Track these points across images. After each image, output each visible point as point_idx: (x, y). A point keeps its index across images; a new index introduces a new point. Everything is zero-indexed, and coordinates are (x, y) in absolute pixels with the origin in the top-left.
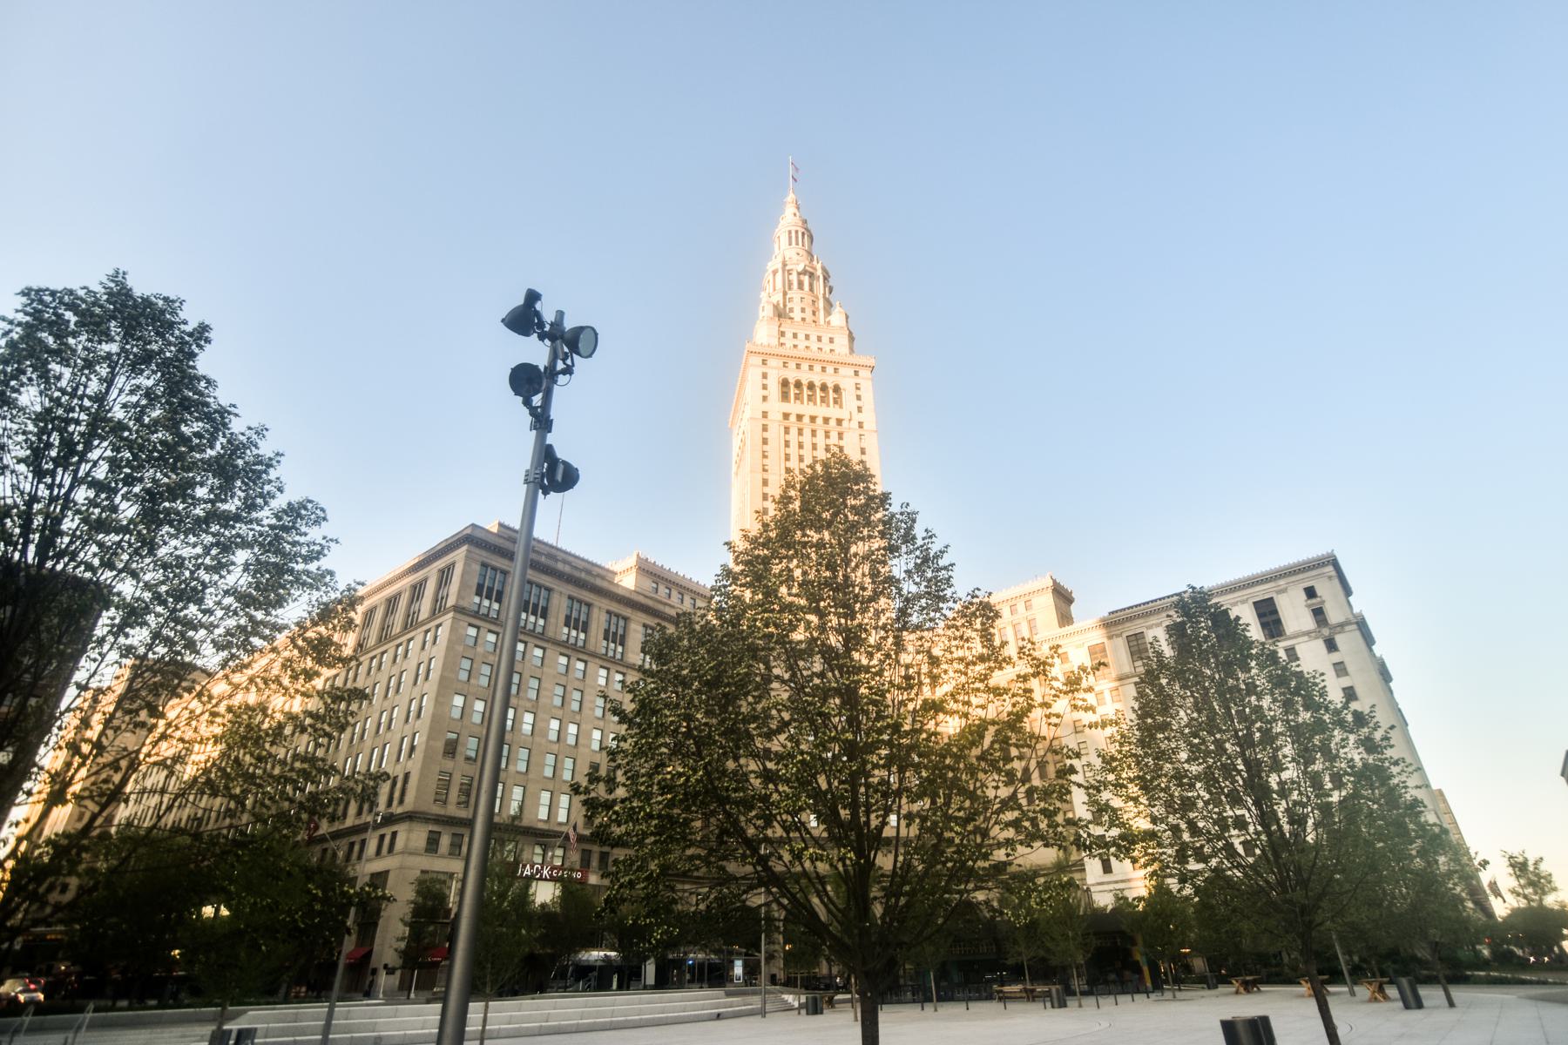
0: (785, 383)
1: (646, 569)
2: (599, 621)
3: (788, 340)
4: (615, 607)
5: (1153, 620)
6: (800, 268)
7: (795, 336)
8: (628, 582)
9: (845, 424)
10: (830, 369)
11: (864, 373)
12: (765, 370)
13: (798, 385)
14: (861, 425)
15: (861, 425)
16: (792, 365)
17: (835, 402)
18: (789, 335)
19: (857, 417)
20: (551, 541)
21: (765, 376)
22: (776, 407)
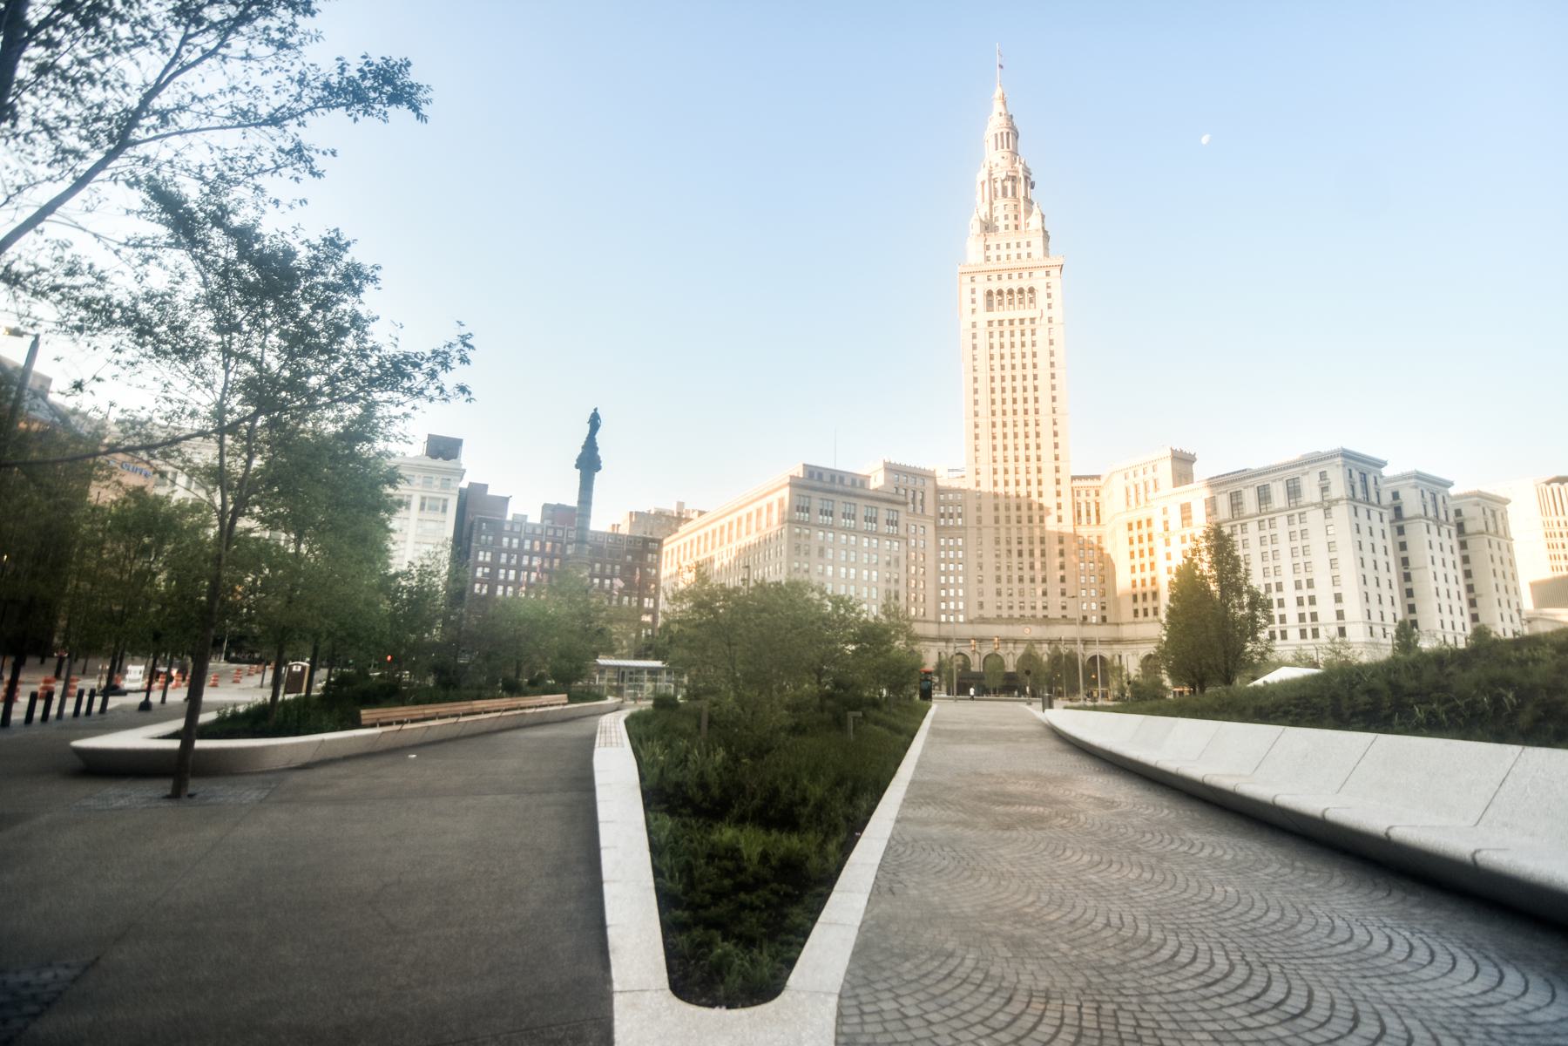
0: (990, 293)
1: (890, 468)
2: (861, 512)
3: (993, 253)
4: (869, 503)
7: (998, 247)
8: (877, 481)
10: (1025, 275)
11: (1055, 272)
12: (973, 285)
13: (1000, 293)
14: (1050, 320)
15: (1050, 320)
17: (1031, 301)
18: (993, 247)
19: (1047, 314)
20: (832, 467)
21: (973, 291)
22: (982, 316)
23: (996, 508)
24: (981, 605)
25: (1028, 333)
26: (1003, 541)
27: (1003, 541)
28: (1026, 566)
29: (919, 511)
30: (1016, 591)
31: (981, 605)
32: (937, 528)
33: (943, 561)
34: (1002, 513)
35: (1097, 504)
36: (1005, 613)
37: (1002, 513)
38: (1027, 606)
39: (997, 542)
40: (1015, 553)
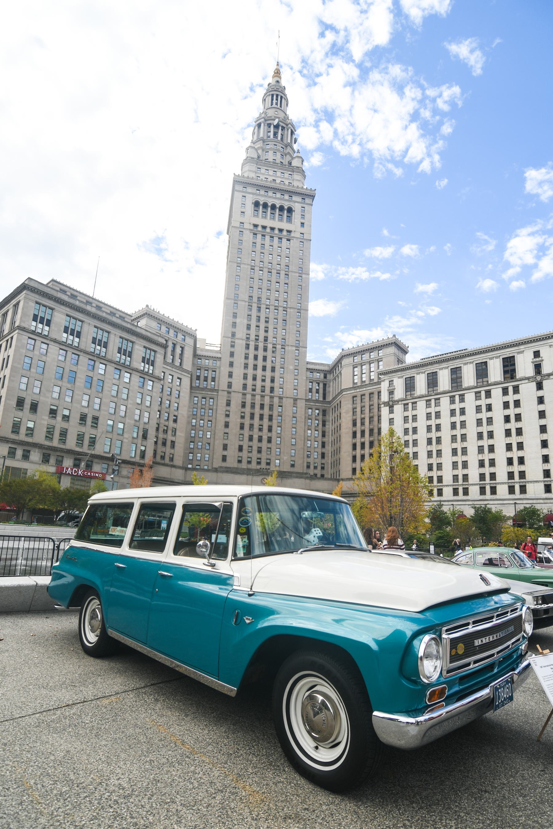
0: (257, 204)
5: (444, 365)
6: (276, 122)
9: (293, 234)
13: (265, 205)
16: (262, 192)
18: (263, 171)
23: (245, 377)
24: (224, 458)
25: (284, 240)
26: (248, 405)
27: (248, 405)
28: (265, 428)
29: (177, 363)
30: (255, 449)
31: (224, 458)
32: (191, 387)
33: (194, 416)
34: (250, 382)
35: (325, 385)
36: (244, 465)
37: (250, 382)
38: (263, 462)
39: (243, 406)
40: (257, 417)
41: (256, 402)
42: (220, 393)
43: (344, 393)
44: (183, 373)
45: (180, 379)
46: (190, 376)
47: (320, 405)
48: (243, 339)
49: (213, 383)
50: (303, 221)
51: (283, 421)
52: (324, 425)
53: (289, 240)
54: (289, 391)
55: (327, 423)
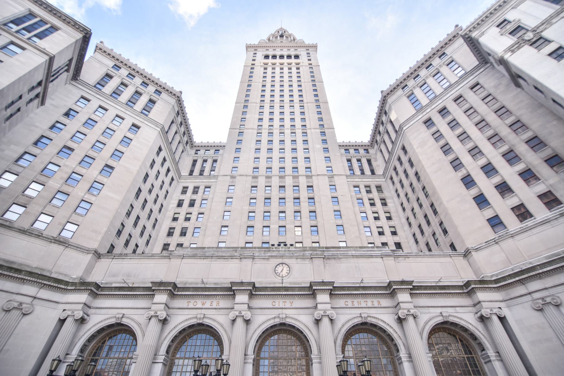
9: (301, 64)
19: (310, 62)
34: (263, 164)
35: (369, 161)
41: (273, 185)
42: (220, 178)
43: (404, 128)
44: (146, 122)
45: (138, 128)
46: (159, 129)
47: (370, 180)
48: (253, 129)
49: (212, 173)
50: (309, 58)
51: (316, 203)
52: (385, 204)
53: (298, 69)
54: (319, 164)
55: (388, 201)
